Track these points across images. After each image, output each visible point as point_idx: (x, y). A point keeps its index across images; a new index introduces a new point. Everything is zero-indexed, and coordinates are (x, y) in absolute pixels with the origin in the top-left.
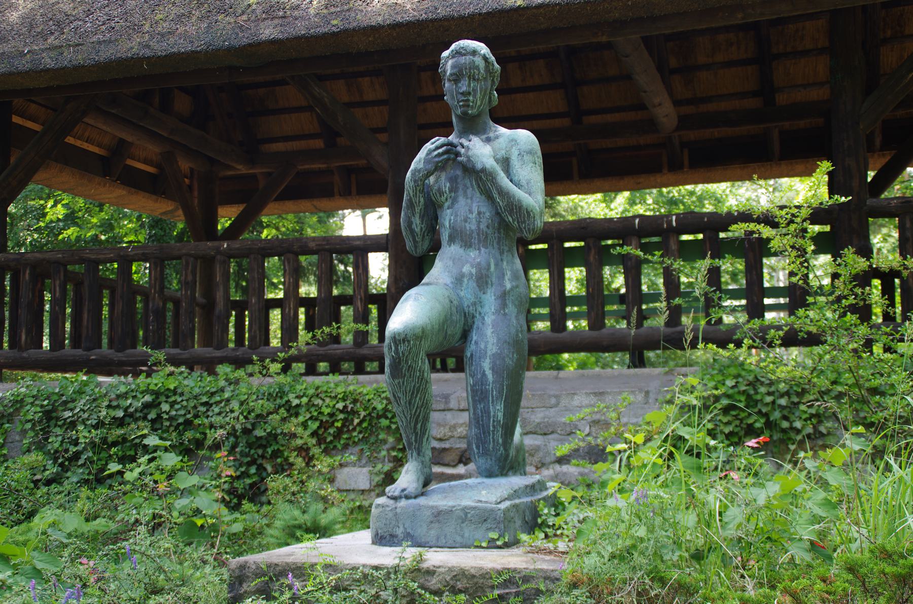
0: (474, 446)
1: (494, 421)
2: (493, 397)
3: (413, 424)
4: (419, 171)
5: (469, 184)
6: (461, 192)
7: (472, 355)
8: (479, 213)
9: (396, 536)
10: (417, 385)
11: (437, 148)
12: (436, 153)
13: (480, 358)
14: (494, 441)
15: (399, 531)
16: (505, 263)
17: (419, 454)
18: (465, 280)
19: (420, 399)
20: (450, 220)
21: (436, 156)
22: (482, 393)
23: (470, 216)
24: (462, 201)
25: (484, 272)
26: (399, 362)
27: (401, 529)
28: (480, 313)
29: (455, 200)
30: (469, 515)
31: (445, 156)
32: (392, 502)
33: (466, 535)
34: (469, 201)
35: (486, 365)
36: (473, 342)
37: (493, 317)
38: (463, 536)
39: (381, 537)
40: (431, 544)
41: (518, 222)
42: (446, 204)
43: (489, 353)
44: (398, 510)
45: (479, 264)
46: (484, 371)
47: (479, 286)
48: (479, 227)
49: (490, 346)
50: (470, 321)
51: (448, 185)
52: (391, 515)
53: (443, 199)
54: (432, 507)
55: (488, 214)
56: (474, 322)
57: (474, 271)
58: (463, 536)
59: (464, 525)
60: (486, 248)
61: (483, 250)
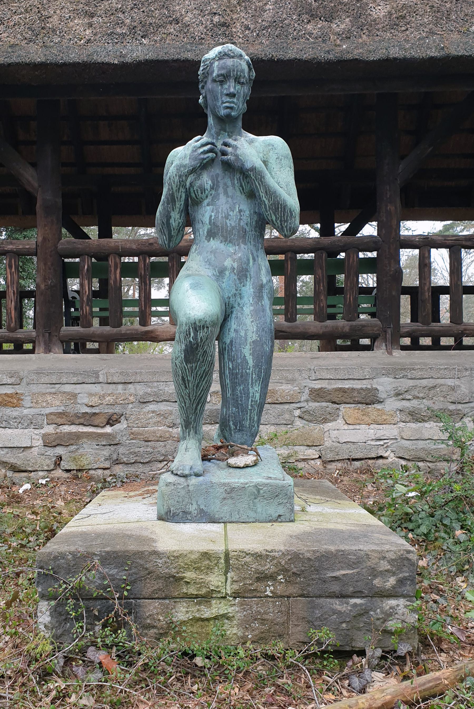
0: (231, 423)
1: (252, 401)
2: (252, 380)
3: (194, 405)
4: (185, 166)
5: (229, 183)
6: (221, 190)
7: (231, 342)
8: (240, 211)
9: (190, 513)
10: (207, 369)
11: (203, 145)
12: (201, 150)
13: (240, 344)
14: (250, 419)
15: (193, 508)
16: (260, 259)
17: (196, 433)
18: (227, 273)
19: (206, 383)
20: (211, 216)
21: (202, 153)
22: (242, 376)
23: (231, 213)
24: (222, 199)
25: (244, 266)
26: (197, 348)
27: (195, 506)
28: (239, 304)
29: (216, 197)
30: (262, 492)
31: (210, 155)
32: (182, 480)
33: (259, 510)
34: (230, 199)
35: (247, 352)
36: (232, 330)
37: (252, 308)
38: (256, 512)
39: (174, 514)
40: (225, 519)
41: (281, 221)
42: (206, 202)
43: (249, 340)
44: (191, 488)
45: (240, 258)
46: (245, 356)
47: (239, 279)
48: (239, 225)
49: (250, 334)
50: (228, 311)
51: (210, 182)
52: (183, 493)
53: (204, 195)
54: (224, 484)
55: (247, 213)
56: (232, 312)
57: (235, 265)
58: (256, 512)
59: (256, 501)
60: (245, 244)
61: (242, 246)
